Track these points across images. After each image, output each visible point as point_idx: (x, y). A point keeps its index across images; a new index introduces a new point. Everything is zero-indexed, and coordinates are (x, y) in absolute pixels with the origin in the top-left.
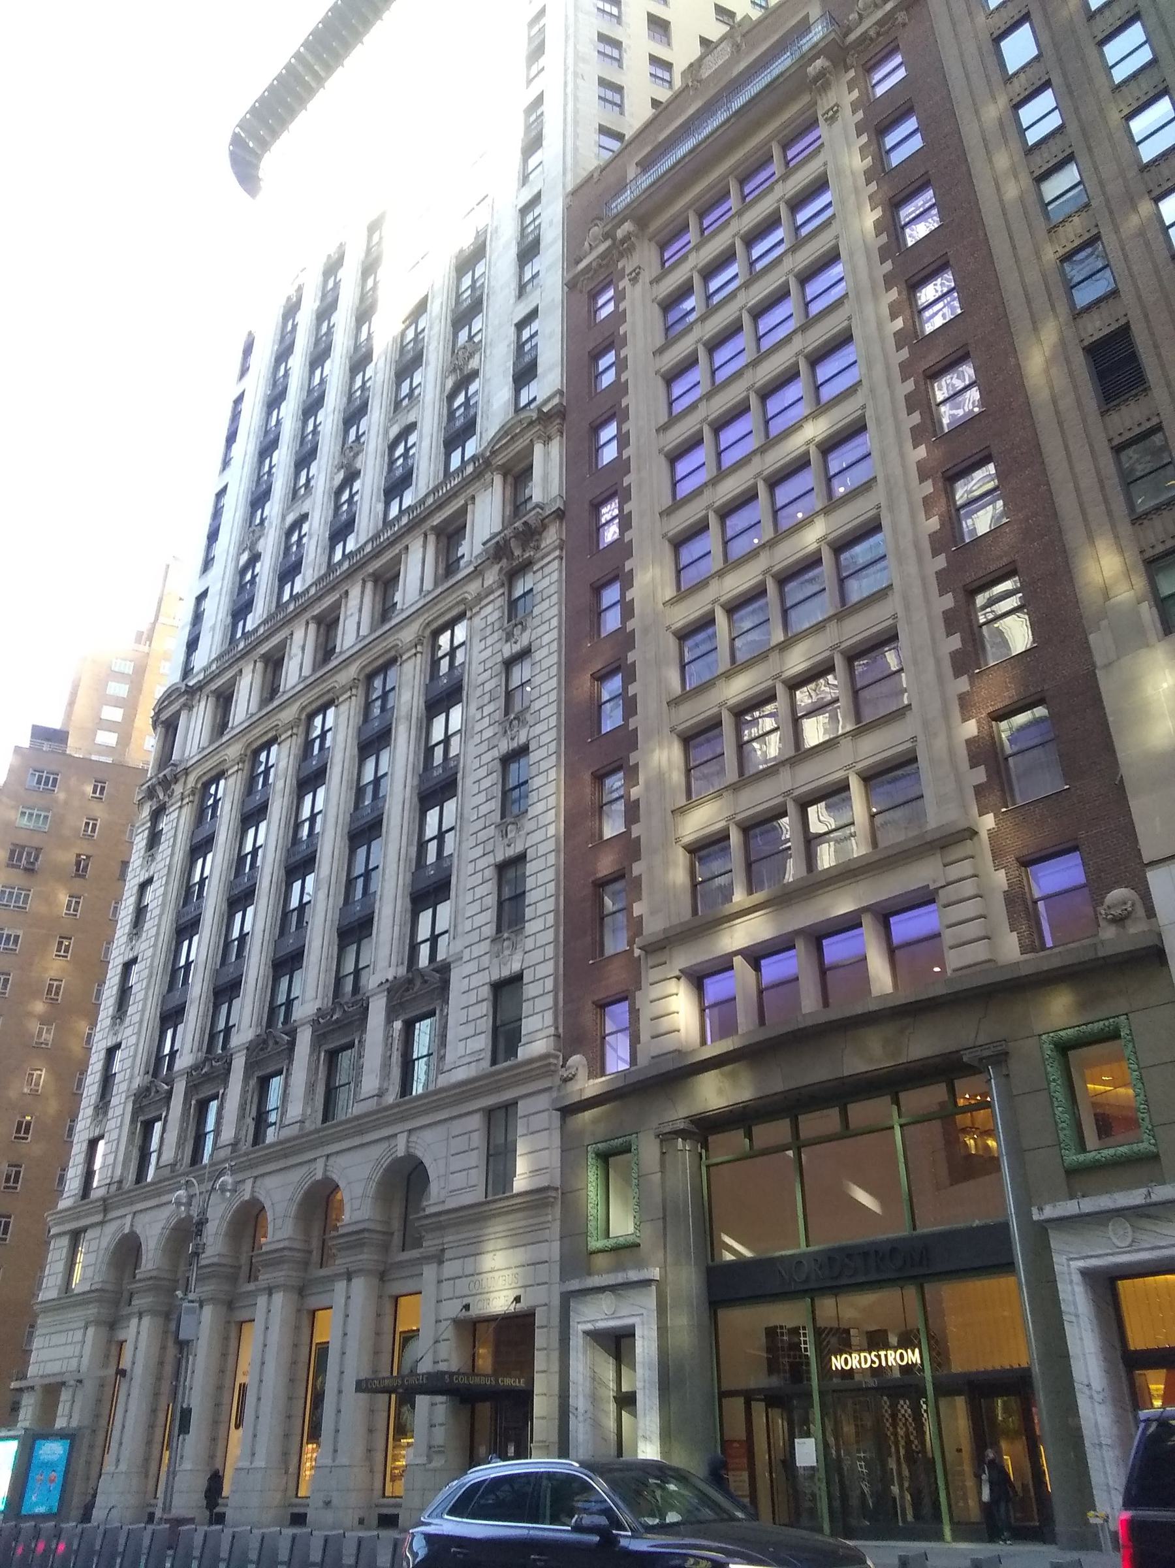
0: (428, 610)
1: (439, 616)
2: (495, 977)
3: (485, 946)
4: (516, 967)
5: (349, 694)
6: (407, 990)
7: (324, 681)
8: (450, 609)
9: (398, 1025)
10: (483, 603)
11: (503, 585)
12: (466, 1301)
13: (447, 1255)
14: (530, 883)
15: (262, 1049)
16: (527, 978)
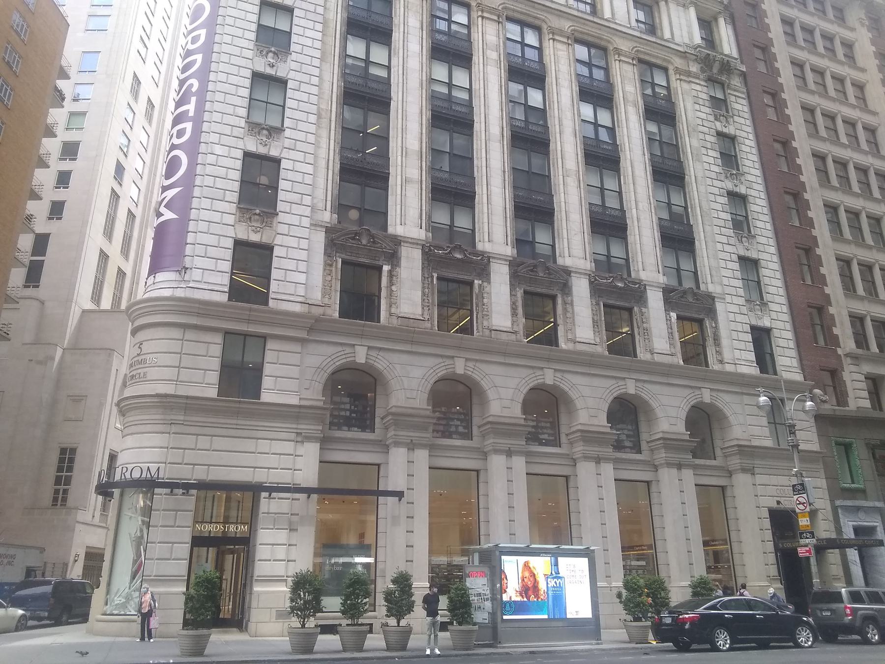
0: (640, 43)
1: (648, 54)
2: (754, 323)
3: (741, 301)
4: (766, 323)
5: (565, 40)
6: (682, 297)
7: (534, 7)
8: (657, 57)
9: (674, 315)
10: (691, 79)
11: (706, 81)
12: (778, 499)
13: (757, 470)
14: (766, 280)
15: (532, 271)
16: (775, 333)
